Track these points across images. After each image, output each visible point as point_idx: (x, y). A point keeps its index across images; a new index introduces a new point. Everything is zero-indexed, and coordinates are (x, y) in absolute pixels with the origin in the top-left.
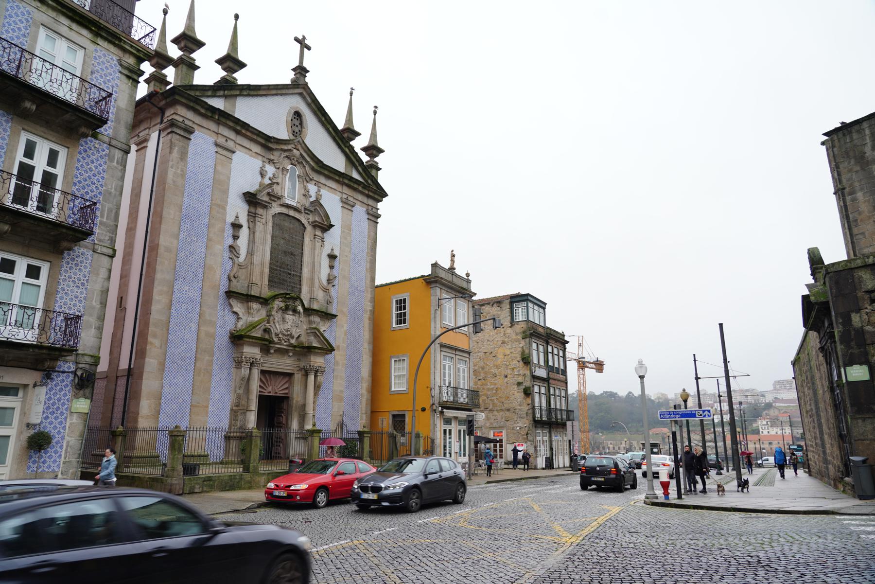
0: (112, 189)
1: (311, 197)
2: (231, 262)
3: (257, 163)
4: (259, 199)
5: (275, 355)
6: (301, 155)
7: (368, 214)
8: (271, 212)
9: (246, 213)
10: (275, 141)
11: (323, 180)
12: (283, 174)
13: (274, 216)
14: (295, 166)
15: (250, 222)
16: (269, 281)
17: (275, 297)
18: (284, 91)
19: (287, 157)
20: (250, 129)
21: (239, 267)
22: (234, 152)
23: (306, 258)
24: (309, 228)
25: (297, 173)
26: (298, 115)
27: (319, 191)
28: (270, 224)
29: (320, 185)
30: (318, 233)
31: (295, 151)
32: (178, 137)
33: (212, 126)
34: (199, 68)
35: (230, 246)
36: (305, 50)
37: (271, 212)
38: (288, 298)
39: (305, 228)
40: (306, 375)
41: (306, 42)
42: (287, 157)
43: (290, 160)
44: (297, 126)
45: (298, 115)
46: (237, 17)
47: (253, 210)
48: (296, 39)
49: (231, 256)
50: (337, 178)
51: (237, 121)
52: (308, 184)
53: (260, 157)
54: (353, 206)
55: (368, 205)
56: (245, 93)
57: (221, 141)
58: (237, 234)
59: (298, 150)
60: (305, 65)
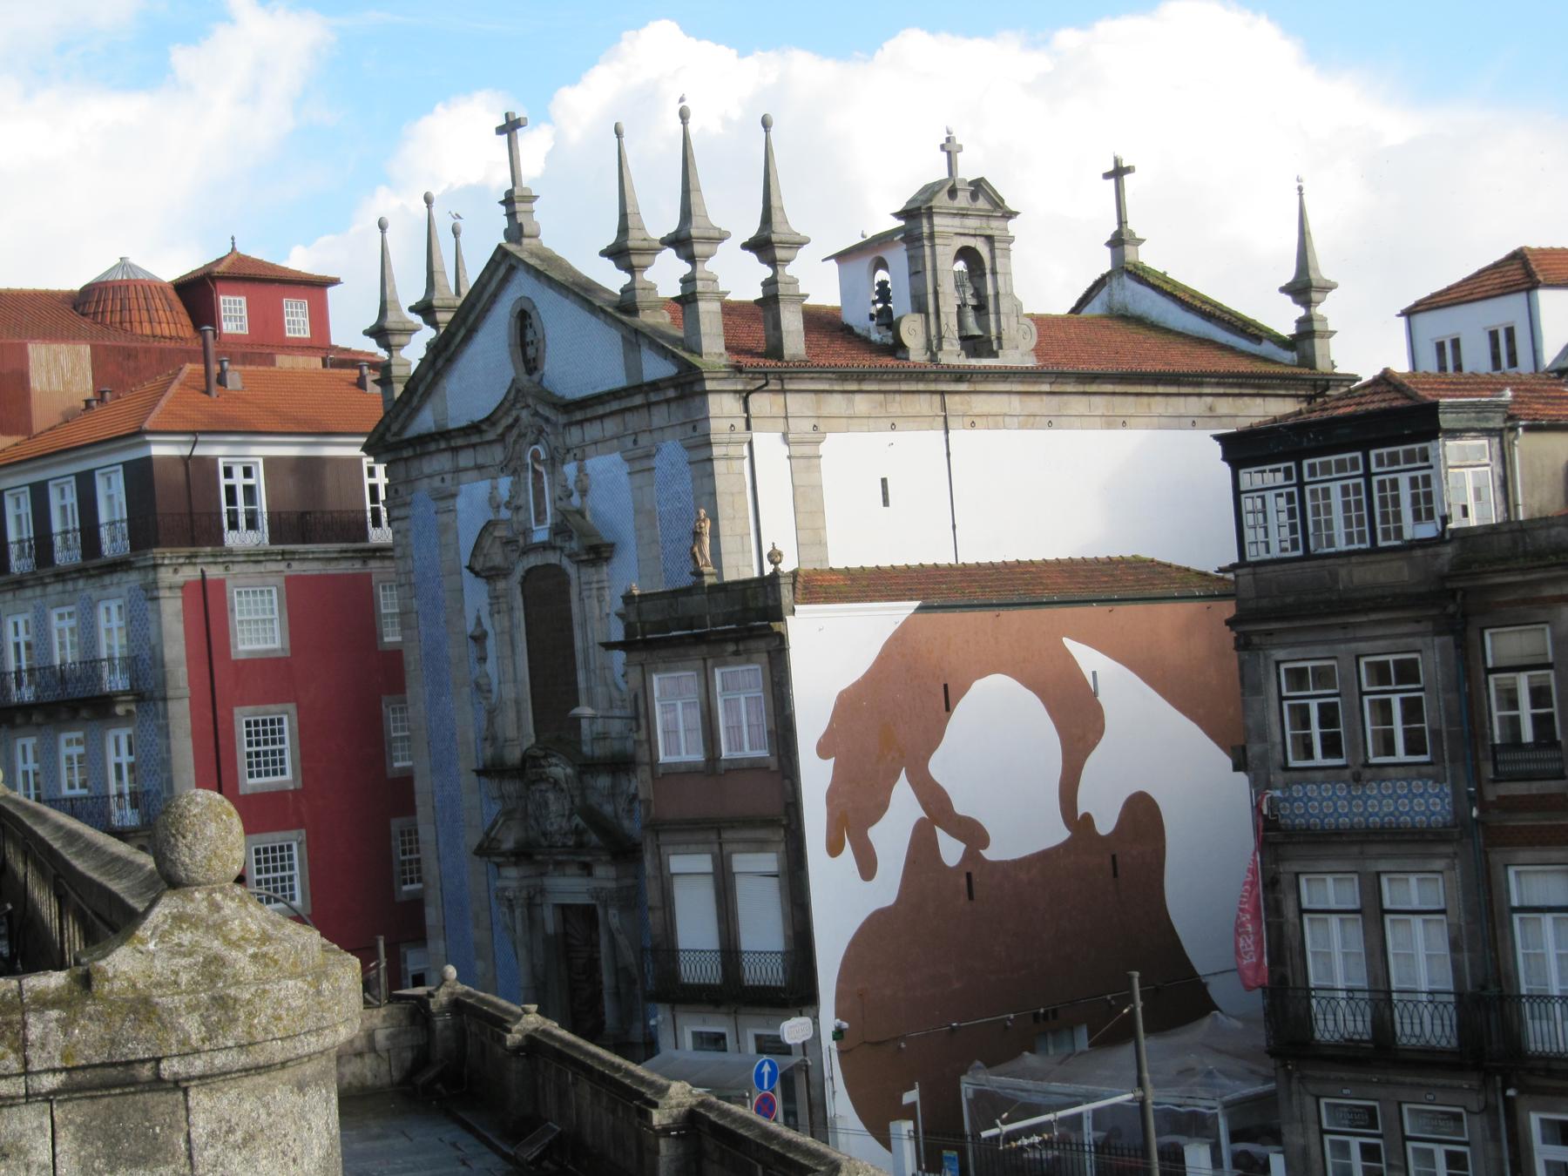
6: (536, 414)
7: (688, 448)
14: (536, 444)
22: (453, 496)
23: (578, 644)
26: (524, 318)
45: (524, 318)
54: (649, 456)
55: (684, 423)
56: (440, 363)
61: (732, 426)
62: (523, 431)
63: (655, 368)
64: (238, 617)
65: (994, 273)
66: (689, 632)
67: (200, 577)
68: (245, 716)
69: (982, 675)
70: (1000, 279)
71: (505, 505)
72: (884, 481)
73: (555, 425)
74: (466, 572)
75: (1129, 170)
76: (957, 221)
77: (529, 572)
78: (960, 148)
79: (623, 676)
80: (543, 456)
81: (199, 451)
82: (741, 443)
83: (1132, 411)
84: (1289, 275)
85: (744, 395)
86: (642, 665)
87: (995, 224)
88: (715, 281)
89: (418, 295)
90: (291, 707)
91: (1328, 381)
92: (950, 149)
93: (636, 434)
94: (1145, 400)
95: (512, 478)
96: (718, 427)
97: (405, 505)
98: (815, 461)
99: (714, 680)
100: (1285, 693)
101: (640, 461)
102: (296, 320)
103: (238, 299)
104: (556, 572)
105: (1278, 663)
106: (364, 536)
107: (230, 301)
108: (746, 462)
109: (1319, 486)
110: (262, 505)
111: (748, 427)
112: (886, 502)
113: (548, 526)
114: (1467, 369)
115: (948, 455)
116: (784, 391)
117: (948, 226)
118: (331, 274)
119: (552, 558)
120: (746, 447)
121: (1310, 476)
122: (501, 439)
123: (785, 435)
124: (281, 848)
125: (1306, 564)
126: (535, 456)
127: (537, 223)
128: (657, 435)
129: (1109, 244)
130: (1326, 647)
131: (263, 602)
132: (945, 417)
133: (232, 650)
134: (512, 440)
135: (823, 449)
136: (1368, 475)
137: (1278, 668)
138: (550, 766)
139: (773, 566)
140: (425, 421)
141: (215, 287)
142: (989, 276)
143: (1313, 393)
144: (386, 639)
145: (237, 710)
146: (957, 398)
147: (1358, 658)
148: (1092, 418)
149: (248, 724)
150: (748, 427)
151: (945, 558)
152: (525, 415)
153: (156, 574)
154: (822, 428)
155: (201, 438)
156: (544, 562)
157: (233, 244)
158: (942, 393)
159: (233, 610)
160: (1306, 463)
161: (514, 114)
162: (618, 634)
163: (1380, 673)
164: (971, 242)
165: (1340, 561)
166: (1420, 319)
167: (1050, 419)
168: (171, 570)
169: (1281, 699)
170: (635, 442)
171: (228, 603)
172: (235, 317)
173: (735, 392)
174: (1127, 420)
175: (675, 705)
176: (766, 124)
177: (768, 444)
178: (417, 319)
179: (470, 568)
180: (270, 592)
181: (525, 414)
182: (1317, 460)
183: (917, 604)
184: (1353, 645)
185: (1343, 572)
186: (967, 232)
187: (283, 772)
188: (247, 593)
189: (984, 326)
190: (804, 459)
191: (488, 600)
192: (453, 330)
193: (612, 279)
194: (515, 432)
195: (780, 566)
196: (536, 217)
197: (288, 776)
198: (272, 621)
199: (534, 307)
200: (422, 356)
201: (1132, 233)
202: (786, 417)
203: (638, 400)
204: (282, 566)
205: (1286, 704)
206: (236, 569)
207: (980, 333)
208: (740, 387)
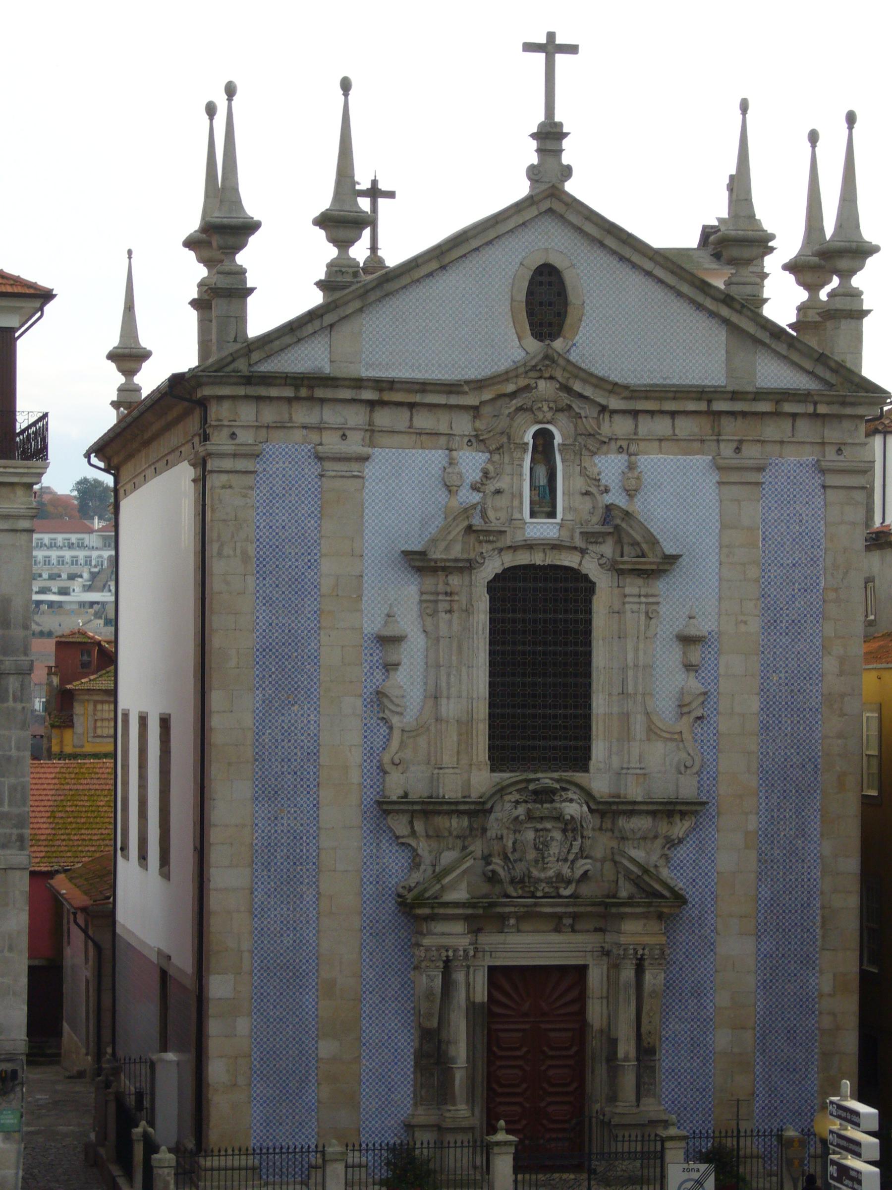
0: (10, 750)
1: (607, 491)
2: (384, 730)
3: (436, 457)
4: (436, 561)
5: (525, 926)
7: (823, 471)
8: (484, 574)
9: (417, 598)
12: (512, 459)
14: (548, 423)
15: (429, 620)
16: (491, 748)
17: (501, 791)
18: (492, 234)
19: (520, 409)
20: (398, 386)
21: (406, 735)
22: (365, 459)
24: (603, 581)
25: (558, 440)
27: (631, 467)
28: (483, 604)
29: (642, 445)
31: (542, 384)
32: (224, 478)
33: (302, 415)
34: (255, 288)
35: (378, 693)
36: (559, 58)
38: (535, 792)
39: (594, 583)
40: (615, 967)
41: (559, 41)
42: (520, 409)
43: (533, 413)
44: (550, 304)
46: (346, 85)
47: (430, 582)
48: (529, 47)
49: (381, 715)
51: (358, 383)
52: (596, 459)
53: (443, 440)
54: (760, 469)
57: (331, 443)
58: (393, 658)
59: (551, 378)
60: (557, 119)
93: (741, 442)
95: (487, 455)
113: (558, 520)
119: (569, 560)
128: (768, 448)
134: (507, 412)
138: (564, 801)
156: (548, 562)
170: (738, 450)
181: (544, 387)
192: (420, 261)
199: (573, 266)
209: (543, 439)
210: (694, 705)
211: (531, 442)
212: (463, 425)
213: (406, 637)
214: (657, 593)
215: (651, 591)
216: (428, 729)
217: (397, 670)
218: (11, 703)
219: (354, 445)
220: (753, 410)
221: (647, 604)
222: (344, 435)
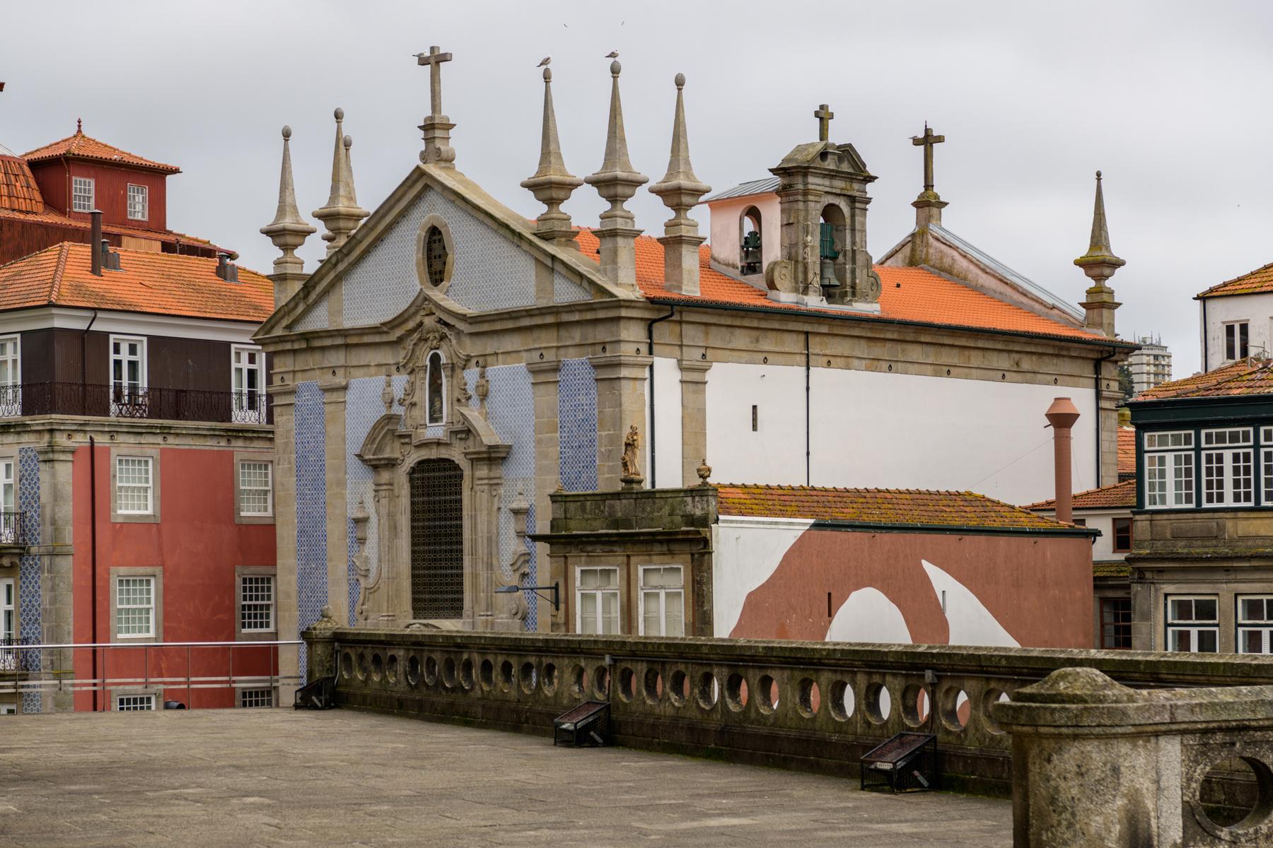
7: (596, 367)
8: (404, 469)
10: (389, 326)
11: (490, 345)
13: (413, 470)
14: (438, 349)
16: (414, 600)
19: (420, 339)
22: (345, 388)
26: (434, 236)
29: (489, 359)
30: (483, 471)
37: (404, 469)
44: (440, 256)
45: (434, 236)
48: (423, 61)
50: (510, 325)
53: (383, 369)
54: (556, 370)
57: (329, 380)
58: (359, 535)
61: (638, 350)
62: (425, 336)
63: (565, 293)
64: (119, 484)
65: (853, 230)
66: (615, 531)
67: (89, 445)
68: (119, 576)
69: (858, 587)
70: (858, 235)
71: (399, 400)
72: (755, 407)
73: (459, 333)
74: (353, 463)
75: (940, 139)
76: (827, 182)
77: (420, 463)
78: (831, 116)
79: (512, 565)
80: (444, 360)
81: (94, 328)
82: (643, 366)
83: (955, 361)
84: (1082, 249)
85: (649, 322)
86: (566, 557)
87: (856, 186)
88: (632, 219)
89: (320, 200)
90: (158, 570)
91: (1114, 347)
92: (823, 116)
94: (966, 353)
96: (627, 351)
97: (293, 392)
98: (701, 386)
99: (637, 574)
100: (1240, 621)
101: (544, 373)
102: (138, 207)
103: (87, 180)
104: (448, 464)
105: (1166, 595)
106: (228, 418)
107: (80, 181)
108: (647, 383)
109: (1214, 452)
110: (143, 382)
111: (651, 353)
112: (755, 428)
113: (444, 423)
114: (1252, 352)
115: (808, 389)
116: (680, 322)
117: (819, 185)
118: (171, 163)
119: (443, 453)
120: (647, 370)
121: (1207, 443)
122: (400, 340)
123: (680, 361)
124: (142, 700)
125: (1198, 515)
126: (435, 359)
127: (452, 150)
129: (916, 204)
130: (1211, 585)
131: (140, 470)
132: (808, 355)
133: (112, 514)
135: (709, 376)
136: (1257, 447)
137: (1166, 599)
139: (701, 480)
140: (319, 320)
141: (69, 169)
142: (848, 232)
143: (1100, 356)
144: (242, 514)
145: (113, 569)
146: (818, 339)
147: (1236, 595)
148: (923, 366)
149: (245, 581)
150: (651, 353)
151: (798, 481)
152: (429, 322)
153: (52, 438)
154: (708, 358)
155: (100, 315)
157: (79, 126)
158: (807, 333)
159: (115, 476)
160: (1203, 432)
161: (438, 48)
162: (543, 527)
163: (1183, 610)
164: (836, 201)
165: (1228, 515)
166: (1211, 305)
167: (891, 363)
168: (65, 435)
169: (1167, 625)
171: (112, 469)
172: (80, 196)
173: (642, 319)
174: (952, 370)
175: (658, 594)
176: (680, 82)
177: (666, 369)
178: (321, 228)
179: (359, 456)
180: (146, 462)
182: (1214, 431)
183: (812, 521)
184: (1233, 585)
185: (1229, 525)
186: (834, 191)
187: (268, 626)
188: (127, 461)
189: (840, 274)
190: (693, 382)
191: (374, 487)
193: (528, 210)
194: (416, 336)
195: (708, 480)
196: (452, 143)
197: (152, 634)
198: (146, 489)
200: (325, 257)
201: (937, 197)
202: (681, 346)
203: (549, 319)
204: (159, 439)
205: (1170, 630)
206: (120, 438)
207: (837, 283)
208: (647, 315)
209: (435, 359)
210: (519, 564)
211: (428, 363)
212: (387, 356)
213: (369, 518)
214: (498, 476)
215: (492, 475)
216: (379, 588)
217: (364, 543)
218: (46, 574)
219: (340, 380)
220: (517, 326)
221: (491, 485)
222: (334, 372)
